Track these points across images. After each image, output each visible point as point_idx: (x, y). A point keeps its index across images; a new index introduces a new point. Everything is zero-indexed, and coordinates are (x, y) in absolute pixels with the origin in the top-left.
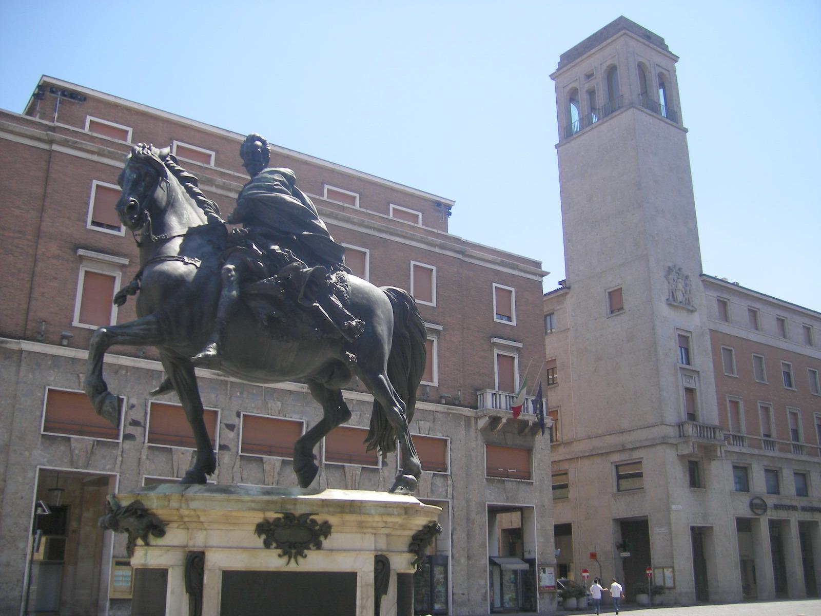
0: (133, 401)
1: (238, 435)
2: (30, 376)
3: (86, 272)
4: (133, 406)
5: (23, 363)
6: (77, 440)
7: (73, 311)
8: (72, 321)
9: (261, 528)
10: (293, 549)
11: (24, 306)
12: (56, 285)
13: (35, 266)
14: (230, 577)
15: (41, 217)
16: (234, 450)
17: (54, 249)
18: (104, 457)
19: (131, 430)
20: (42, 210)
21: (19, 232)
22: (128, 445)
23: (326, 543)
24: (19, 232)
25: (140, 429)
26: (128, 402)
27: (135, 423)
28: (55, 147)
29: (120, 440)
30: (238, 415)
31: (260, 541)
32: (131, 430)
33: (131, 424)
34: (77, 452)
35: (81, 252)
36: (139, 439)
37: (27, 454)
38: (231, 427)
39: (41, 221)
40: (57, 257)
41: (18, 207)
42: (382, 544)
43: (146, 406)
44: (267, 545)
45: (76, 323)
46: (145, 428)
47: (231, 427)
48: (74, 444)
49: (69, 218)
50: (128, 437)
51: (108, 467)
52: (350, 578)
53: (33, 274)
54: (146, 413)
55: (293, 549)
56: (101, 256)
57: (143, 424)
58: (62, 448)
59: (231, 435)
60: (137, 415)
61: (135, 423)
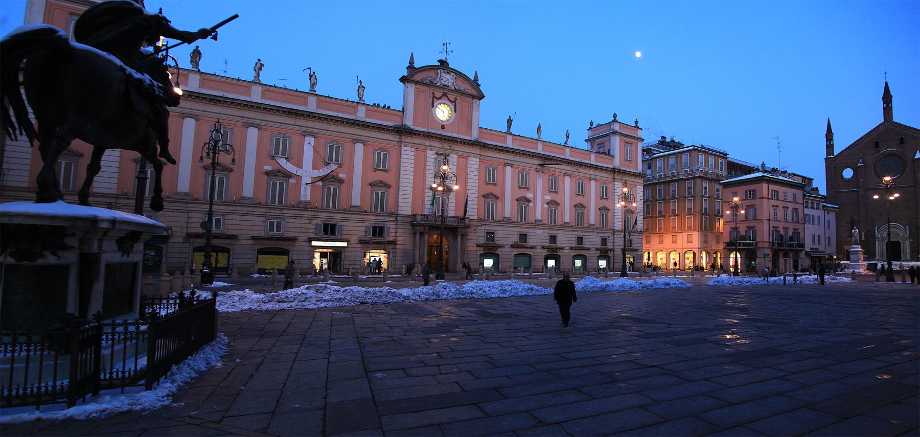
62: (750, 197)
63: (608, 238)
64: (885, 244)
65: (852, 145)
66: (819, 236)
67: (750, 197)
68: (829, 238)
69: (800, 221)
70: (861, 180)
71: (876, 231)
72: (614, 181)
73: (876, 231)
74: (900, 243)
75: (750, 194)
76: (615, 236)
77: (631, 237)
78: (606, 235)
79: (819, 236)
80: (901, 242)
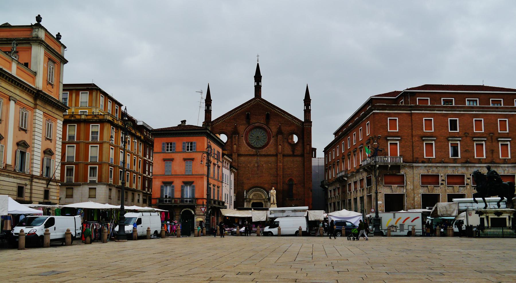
0: (442, 175)
1: (471, 180)
2: (416, 172)
3: (425, 143)
4: (442, 176)
5: (414, 169)
6: (429, 186)
7: (424, 154)
8: (424, 157)
9: (494, 214)
10: (498, 216)
11: (412, 155)
12: (418, 148)
13: (413, 144)
14: (491, 218)
15: (412, 131)
16: (470, 185)
17: (417, 139)
18: (436, 190)
19: (442, 182)
20: (412, 129)
21: (408, 136)
22: (442, 186)
23: (502, 215)
24: (408, 136)
25: (444, 182)
26: (440, 175)
27: (443, 180)
28: (412, 112)
29: (440, 185)
30: (470, 175)
31: (494, 215)
32: (442, 182)
33: (442, 181)
34: (430, 189)
35: (424, 139)
36: (445, 184)
37: (418, 191)
38: (469, 179)
39: (412, 132)
40: (418, 141)
41: (406, 130)
42: (509, 215)
43: (445, 175)
44: (495, 215)
45: (425, 157)
46: (445, 181)
47: (469, 179)
48: (429, 187)
49: (419, 130)
50: (442, 184)
51: (438, 192)
52: (505, 218)
53: (413, 146)
54: (445, 177)
55: (498, 216)
56: (429, 139)
57: (445, 180)
58: (426, 188)
59: (469, 181)
60: (443, 178)
61: (443, 180)
62: (168, 150)
63: (25, 187)
64: (251, 205)
65: (224, 115)
66: (228, 195)
67: (168, 150)
68: (231, 197)
69: (220, 179)
70: (235, 146)
71: (245, 193)
72: (35, 108)
73: (245, 193)
74: (263, 204)
75: (168, 147)
76: (34, 184)
77: (49, 186)
78: (23, 182)
79: (228, 195)
80: (263, 203)
